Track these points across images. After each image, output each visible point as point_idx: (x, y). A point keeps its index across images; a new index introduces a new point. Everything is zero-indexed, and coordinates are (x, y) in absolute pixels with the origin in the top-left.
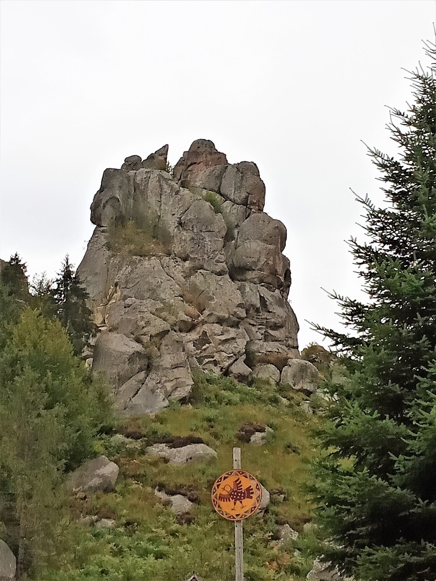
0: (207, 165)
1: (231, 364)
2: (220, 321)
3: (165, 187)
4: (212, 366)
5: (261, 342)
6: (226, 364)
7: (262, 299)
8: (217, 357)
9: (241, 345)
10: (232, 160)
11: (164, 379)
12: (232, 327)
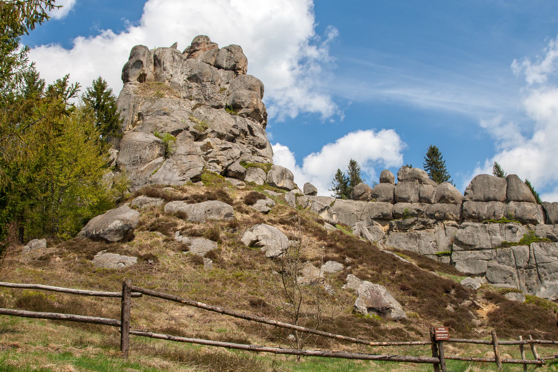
0: (205, 50)
1: (230, 165)
2: (221, 136)
3: (177, 57)
4: (215, 164)
6: (227, 164)
7: (249, 127)
8: (219, 158)
11: (179, 162)
12: (229, 141)
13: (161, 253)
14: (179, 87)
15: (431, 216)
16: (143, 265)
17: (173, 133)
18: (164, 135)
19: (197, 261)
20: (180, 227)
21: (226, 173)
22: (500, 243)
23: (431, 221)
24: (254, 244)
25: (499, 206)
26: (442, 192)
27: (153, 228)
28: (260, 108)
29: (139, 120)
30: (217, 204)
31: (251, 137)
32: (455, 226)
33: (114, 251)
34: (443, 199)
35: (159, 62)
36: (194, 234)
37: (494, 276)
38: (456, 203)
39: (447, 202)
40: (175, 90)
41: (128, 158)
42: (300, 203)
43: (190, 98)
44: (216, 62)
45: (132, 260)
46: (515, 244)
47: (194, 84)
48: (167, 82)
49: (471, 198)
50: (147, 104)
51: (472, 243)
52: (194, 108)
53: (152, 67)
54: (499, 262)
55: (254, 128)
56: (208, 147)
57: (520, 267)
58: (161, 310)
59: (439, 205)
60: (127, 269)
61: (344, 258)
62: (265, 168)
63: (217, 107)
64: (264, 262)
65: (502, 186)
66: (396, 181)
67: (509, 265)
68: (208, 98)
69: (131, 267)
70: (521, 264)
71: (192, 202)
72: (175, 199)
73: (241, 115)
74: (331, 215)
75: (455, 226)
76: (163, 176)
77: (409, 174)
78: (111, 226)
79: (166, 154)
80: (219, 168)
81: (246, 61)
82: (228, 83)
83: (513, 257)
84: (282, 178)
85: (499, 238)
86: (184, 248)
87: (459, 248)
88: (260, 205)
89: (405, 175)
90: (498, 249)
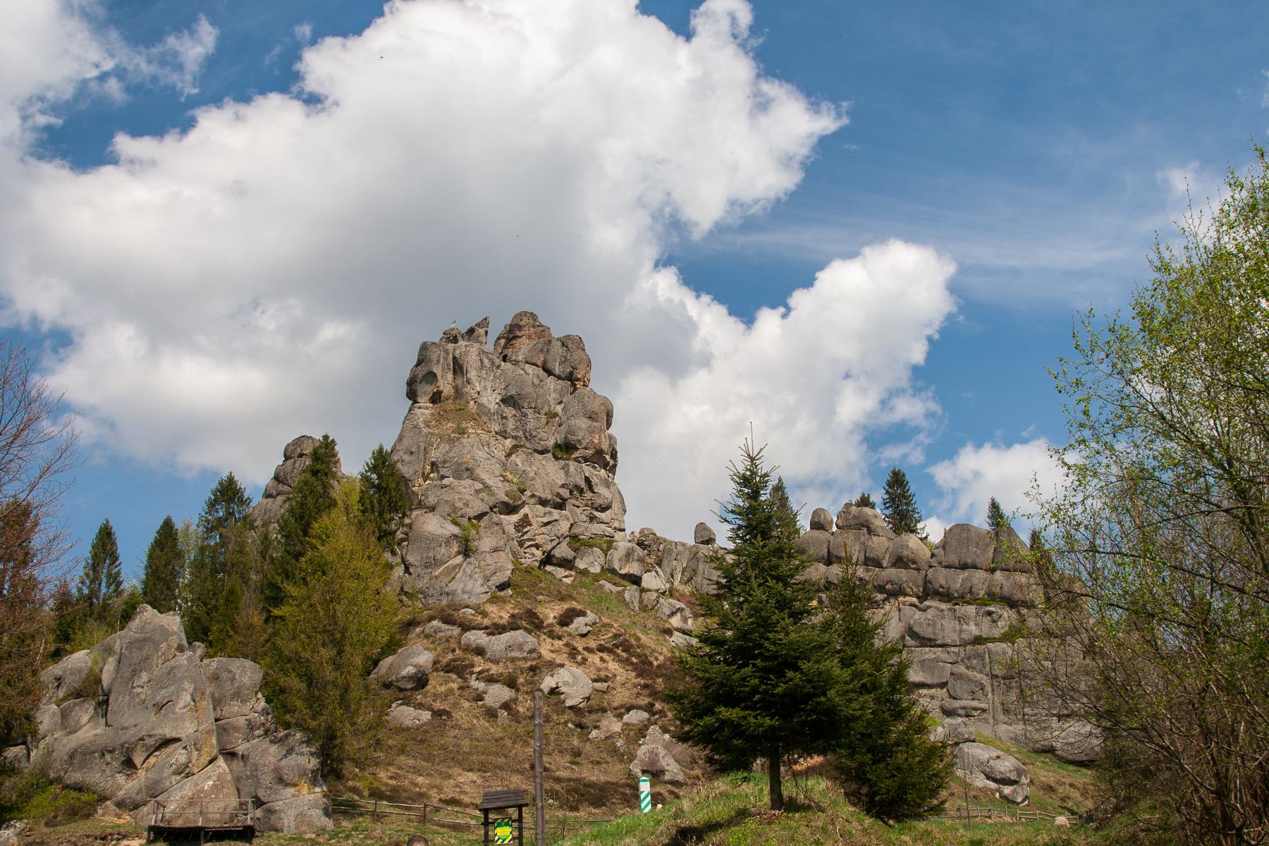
0: (529, 337)
2: (543, 502)
3: (486, 361)
4: (534, 550)
5: (586, 525)
6: (549, 547)
7: (587, 480)
8: (539, 540)
9: (564, 527)
10: (557, 333)
11: (482, 563)
13: (455, 705)
14: (487, 412)
15: (881, 589)
16: (437, 721)
17: (475, 518)
18: (465, 521)
19: (491, 714)
20: (477, 669)
21: (548, 559)
22: (972, 638)
23: (880, 597)
24: (554, 691)
25: (979, 576)
26: (900, 550)
27: (449, 669)
28: (605, 447)
29: (432, 471)
30: (519, 636)
31: (588, 495)
32: (915, 606)
33: (408, 704)
34: (900, 562)
35: (461, 368)
36: (491, 680)
37: (958, 689)
38: (918, 570)
39: (906, 567)
40: (484, 419)
41: (419, 557)
42: (645, 602)
43: (503, 434)
44: (545, 362)
45: (426, 716)
46: (994, 640)
47: (509, 411)
48: (472, 403)
49: (940, 563)
50: (445, 447)
51: (932, 636)
52: (508, 455)
53: (450, 376)
54: (968, 668)
55: (594, 480)
56: (525, 522)
57: (997, 676)
58: (450, 777)
59: (893, 571)
60: (421, 726)
61: (653, 705)
62: (604, 546)
63: (541, 453)
64: (563, 712)
65: (988, 545)
66: (834, 529)
67: (981, 672)
68: (530, 437)
69: (425, 724)
70: (997, 672)
71: (493, 634)
72: (474, 628)
73: (576, 460)
74: (685, 620)
75: (915, 606)
76: (462, 585)
77: (854, 517)
78: (404, 673)
79: (466, 552)
80: (539, 553)
81: (589, 365)
82: (561, 402)
83: (987, 660)
84: (628, 561)
85: (973, 630)
86: (479, 697)
87: (913, 643)
88: (579, 624)
89: (847, 519)
90: (968, 647)
